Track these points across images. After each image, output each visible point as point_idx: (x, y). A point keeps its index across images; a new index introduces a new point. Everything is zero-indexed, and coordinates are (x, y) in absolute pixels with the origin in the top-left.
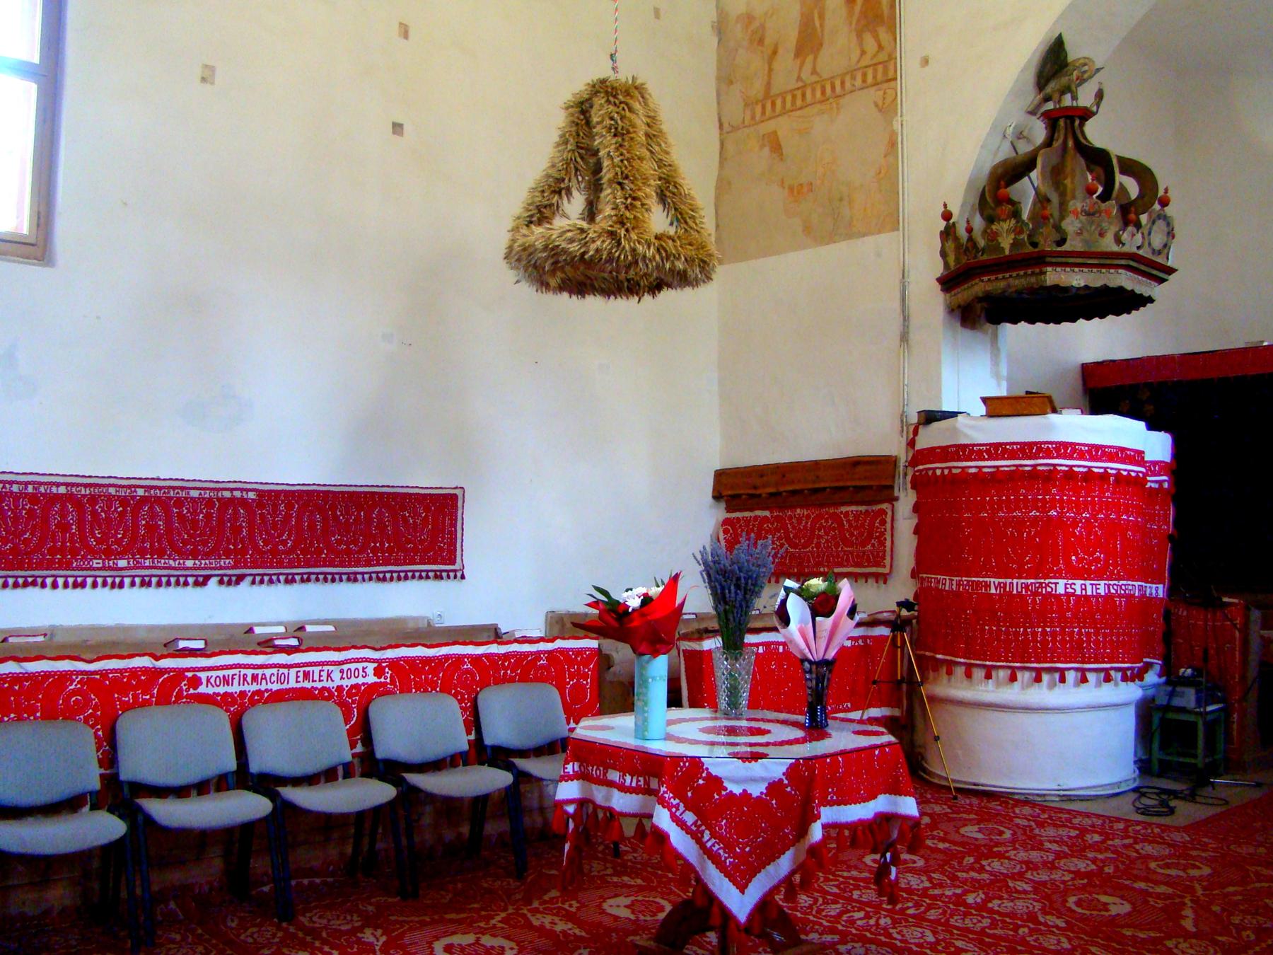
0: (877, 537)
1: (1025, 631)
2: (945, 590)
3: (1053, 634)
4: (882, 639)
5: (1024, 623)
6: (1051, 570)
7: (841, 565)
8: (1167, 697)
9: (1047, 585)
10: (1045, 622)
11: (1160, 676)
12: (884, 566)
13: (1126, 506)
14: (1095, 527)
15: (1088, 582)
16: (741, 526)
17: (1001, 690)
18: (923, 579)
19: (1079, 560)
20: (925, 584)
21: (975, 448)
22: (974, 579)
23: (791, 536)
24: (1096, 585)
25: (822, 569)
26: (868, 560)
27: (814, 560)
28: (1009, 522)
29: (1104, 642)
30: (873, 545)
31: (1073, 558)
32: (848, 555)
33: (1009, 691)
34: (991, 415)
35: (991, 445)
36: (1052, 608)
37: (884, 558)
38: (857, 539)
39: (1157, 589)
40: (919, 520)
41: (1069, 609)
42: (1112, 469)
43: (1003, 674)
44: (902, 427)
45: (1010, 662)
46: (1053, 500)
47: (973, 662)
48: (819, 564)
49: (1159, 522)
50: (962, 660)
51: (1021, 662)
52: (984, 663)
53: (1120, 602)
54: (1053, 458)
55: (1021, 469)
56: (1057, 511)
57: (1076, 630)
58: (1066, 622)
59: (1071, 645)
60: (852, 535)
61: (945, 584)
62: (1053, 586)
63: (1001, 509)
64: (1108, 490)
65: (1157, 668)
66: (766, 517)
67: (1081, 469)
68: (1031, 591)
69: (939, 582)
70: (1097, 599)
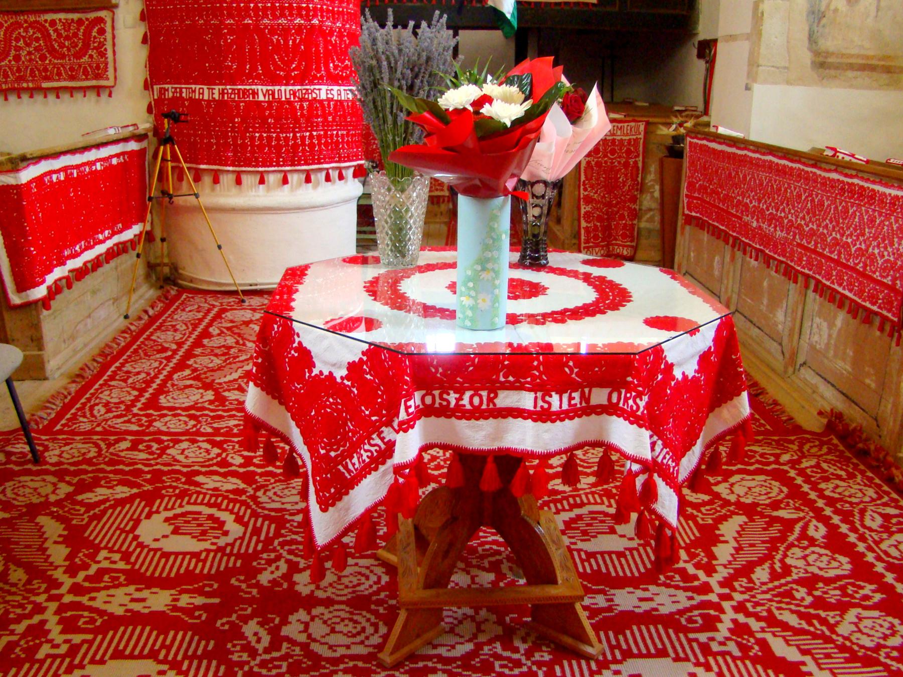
0: (95, 48)
1: (295, 136)
2: (202, 100)
5: (295, 127)
6: (315, 77)
9: (312, 91)
10: (312, 127)
12: (107, 79)
15: (342, 88)
19: (336, 67)
22: (239, 87)
25: (25, 85)
26: (86, 73)
27: (13, 74)
28: (273, 31)
30: (91, 56)
31: (331, 65)
37: (106, 69)
38: (69, 50)
41: (330, 114)
43: (273, 179)
45: (282, 166)
46: (315, 9)
47: (244, 169)
48: (21, 79)
50: (231, 168)
51: (291, 165)
60: (62, 46)
61: (203, 94)
62: (317, 92)
63: (265, 16)
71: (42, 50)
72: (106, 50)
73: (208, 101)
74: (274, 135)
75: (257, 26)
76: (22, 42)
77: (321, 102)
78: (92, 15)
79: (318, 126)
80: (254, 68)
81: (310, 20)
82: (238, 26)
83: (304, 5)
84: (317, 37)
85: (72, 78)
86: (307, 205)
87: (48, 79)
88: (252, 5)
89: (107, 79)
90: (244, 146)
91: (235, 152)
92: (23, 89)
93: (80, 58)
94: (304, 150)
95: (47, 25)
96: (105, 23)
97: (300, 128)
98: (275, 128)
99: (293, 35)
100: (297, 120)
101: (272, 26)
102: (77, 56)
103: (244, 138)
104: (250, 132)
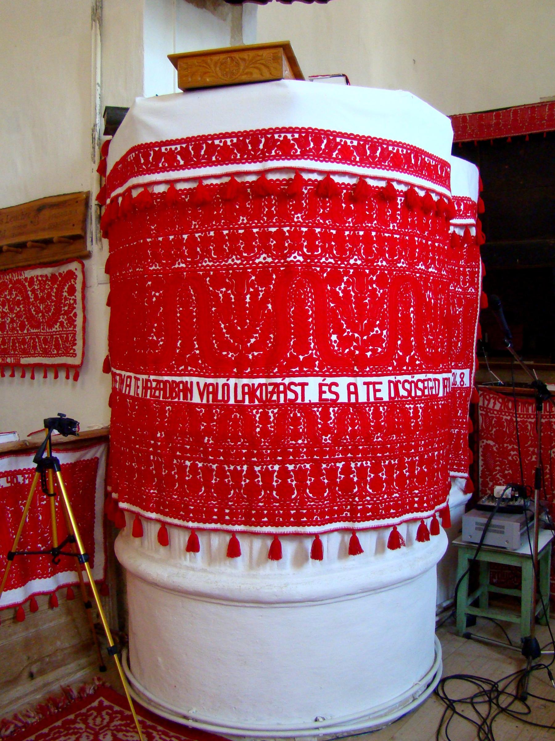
1: (251, 471)
2: (129, 396)
3: (300, 474)
5: (249, 455)
7: (26, 353)
8: (481, 533)
9: (288, 388)
10: (285, 454)
11: (465, 492)
13: (424, 248)
14: (371, 282)
15: (360, 381)
17: (216, 568)
19: (345, 342)
21: (163, 149)
22: (166, 378)
24: (374, 384)
28: (218, 280)
29: (390, 481)
31: (334, 337)
33: (229, 570)
34: (188, 89)
35: (188, 140)
36: (296, 430)
39: (462, 375)
41: (326, 430)
42: (400, 182)
44: (94, 148)
45: (228, 523)
46: (296, 236)
49: (464, 283)
50: (153, 515)
51: (245, 523)
52: (185, 524)
53: (416, 410)
54: (295, 157)
55: (239, 180)
56: (304, 255)
57: (340, 465)
58: (322, 453)
59: (332, 491)
61: (129, 386)
63: (206, 253)
64: (393, 219)
65: (463, 482)
67: (346, 180)
68: (260, 400)
69: (122, 382)
70: (377, 410)
71: (21, 316)
72: (75, 315)
73: (132, 398)
74: (214, 467)
75: (193, 272)
76: (7, 307)
77: (307, 408)
78: (64, 269)
79: (297, 453)
80: (188, 347)
81: (285, 257)
82: (165, 274)
83: (273, 230)
84: (300, 285)
86: (274, 598)
88: (185, 237)
89: (74, 355)
90: (170, 479)
92: (8, 365)
93: (51, 327)
94: (269, 499)
95: (27, 284)
96: (75, 279)
97: (260, 455)
98: (216, 454)
99: (252, 285)
100: (254, 443)
101: (216, 271)
103: (170, 467)
104: (177, 457)
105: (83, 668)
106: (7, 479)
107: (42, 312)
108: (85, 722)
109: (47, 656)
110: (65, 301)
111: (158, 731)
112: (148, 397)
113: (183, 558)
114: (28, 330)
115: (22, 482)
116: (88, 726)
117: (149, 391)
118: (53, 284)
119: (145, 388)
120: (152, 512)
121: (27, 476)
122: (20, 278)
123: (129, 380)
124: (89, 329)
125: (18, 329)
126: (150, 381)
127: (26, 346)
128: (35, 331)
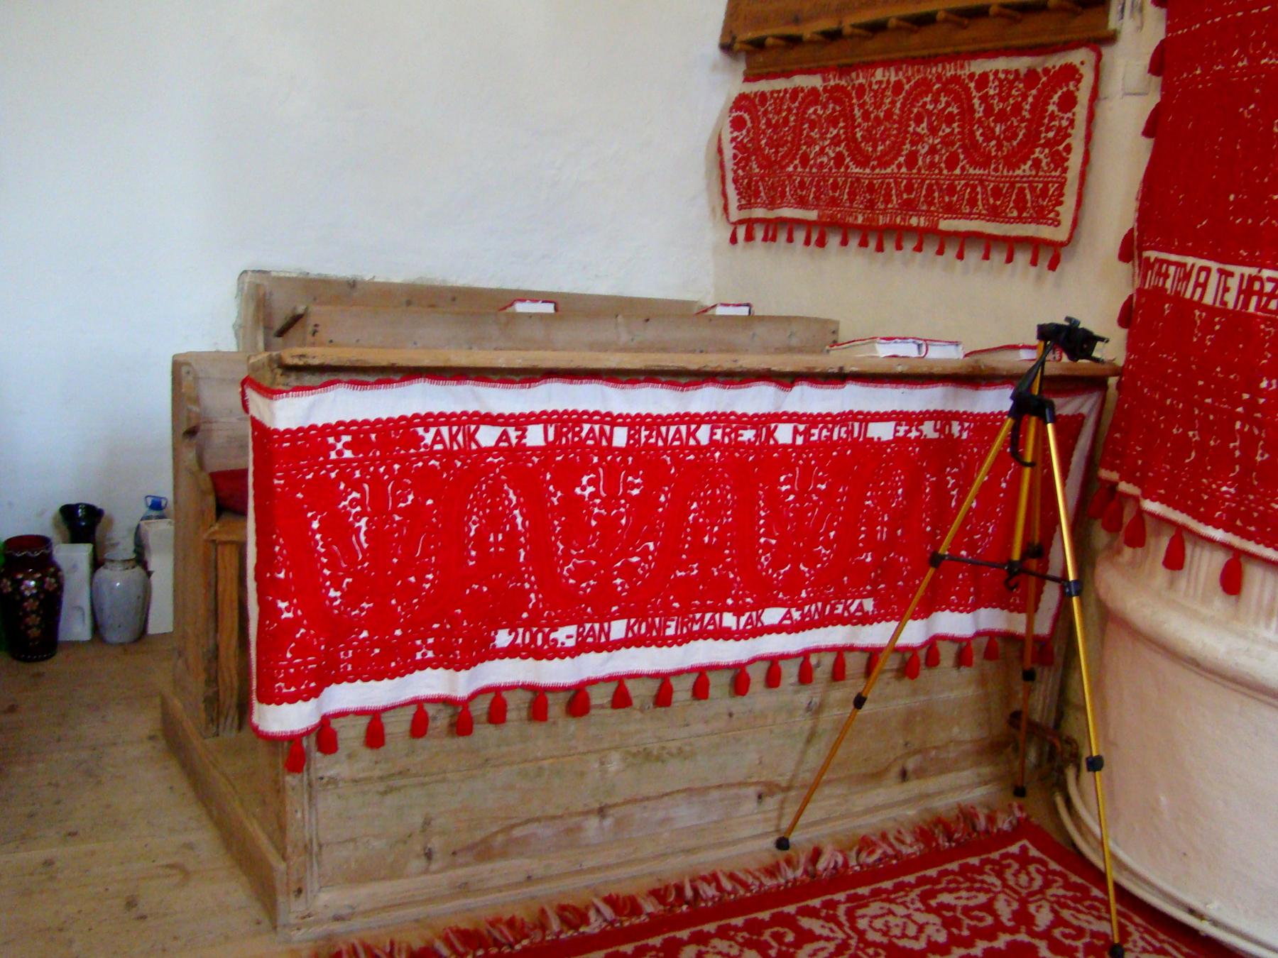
0: (1049, 143)
2: (1199, 305)
4: (984, 425)
12: (1055, 222)
16: (765, 113)
18: (1146, 265)
20: (1152, 281)
23: (859, 135)
25: (914, 221)
26: (1020, 204)
27: (899, 195)
30: (1037, 163)
32: (974, 188)
38: (999, 147)
40: (1163, 97)
47: (1251, 547)
48: (909, 207)
50: (1218, 534)
61: (1204, 286)
66: (814, 91)
69: (1187, 276)
73: (1210, 310)
85: (995, 214)
87: (952, 211)
91: (1242, 484)
102: (1012, 161)
105: (986, 783)
106: (935, 425)
107: (998, 139)
108: (1000, 875)
109: (935, 748)
110: (1050, 121)
111: (1136, 925)
112: (1252, 309)
113: (1262, 624)
114: (963, 169)
115: (957, 434)
116: (1005, 885)
117: (1254, 300)
118: (1029, 86)
119: (1246, 292)
120: (1217, 527)
121: (966, 425)
122: (959, 72)
123: (1203, 275)
124: (1091, 179)
125: (943, 165)
126: (1260, 279)
127: (955, 199)
128: (978, 172)
